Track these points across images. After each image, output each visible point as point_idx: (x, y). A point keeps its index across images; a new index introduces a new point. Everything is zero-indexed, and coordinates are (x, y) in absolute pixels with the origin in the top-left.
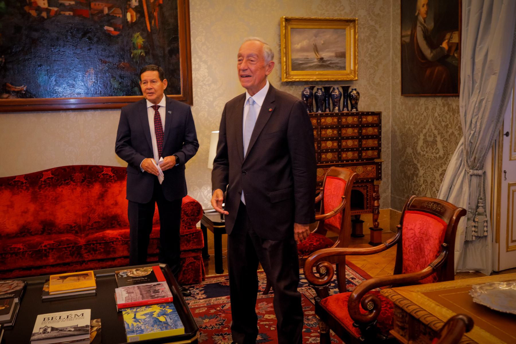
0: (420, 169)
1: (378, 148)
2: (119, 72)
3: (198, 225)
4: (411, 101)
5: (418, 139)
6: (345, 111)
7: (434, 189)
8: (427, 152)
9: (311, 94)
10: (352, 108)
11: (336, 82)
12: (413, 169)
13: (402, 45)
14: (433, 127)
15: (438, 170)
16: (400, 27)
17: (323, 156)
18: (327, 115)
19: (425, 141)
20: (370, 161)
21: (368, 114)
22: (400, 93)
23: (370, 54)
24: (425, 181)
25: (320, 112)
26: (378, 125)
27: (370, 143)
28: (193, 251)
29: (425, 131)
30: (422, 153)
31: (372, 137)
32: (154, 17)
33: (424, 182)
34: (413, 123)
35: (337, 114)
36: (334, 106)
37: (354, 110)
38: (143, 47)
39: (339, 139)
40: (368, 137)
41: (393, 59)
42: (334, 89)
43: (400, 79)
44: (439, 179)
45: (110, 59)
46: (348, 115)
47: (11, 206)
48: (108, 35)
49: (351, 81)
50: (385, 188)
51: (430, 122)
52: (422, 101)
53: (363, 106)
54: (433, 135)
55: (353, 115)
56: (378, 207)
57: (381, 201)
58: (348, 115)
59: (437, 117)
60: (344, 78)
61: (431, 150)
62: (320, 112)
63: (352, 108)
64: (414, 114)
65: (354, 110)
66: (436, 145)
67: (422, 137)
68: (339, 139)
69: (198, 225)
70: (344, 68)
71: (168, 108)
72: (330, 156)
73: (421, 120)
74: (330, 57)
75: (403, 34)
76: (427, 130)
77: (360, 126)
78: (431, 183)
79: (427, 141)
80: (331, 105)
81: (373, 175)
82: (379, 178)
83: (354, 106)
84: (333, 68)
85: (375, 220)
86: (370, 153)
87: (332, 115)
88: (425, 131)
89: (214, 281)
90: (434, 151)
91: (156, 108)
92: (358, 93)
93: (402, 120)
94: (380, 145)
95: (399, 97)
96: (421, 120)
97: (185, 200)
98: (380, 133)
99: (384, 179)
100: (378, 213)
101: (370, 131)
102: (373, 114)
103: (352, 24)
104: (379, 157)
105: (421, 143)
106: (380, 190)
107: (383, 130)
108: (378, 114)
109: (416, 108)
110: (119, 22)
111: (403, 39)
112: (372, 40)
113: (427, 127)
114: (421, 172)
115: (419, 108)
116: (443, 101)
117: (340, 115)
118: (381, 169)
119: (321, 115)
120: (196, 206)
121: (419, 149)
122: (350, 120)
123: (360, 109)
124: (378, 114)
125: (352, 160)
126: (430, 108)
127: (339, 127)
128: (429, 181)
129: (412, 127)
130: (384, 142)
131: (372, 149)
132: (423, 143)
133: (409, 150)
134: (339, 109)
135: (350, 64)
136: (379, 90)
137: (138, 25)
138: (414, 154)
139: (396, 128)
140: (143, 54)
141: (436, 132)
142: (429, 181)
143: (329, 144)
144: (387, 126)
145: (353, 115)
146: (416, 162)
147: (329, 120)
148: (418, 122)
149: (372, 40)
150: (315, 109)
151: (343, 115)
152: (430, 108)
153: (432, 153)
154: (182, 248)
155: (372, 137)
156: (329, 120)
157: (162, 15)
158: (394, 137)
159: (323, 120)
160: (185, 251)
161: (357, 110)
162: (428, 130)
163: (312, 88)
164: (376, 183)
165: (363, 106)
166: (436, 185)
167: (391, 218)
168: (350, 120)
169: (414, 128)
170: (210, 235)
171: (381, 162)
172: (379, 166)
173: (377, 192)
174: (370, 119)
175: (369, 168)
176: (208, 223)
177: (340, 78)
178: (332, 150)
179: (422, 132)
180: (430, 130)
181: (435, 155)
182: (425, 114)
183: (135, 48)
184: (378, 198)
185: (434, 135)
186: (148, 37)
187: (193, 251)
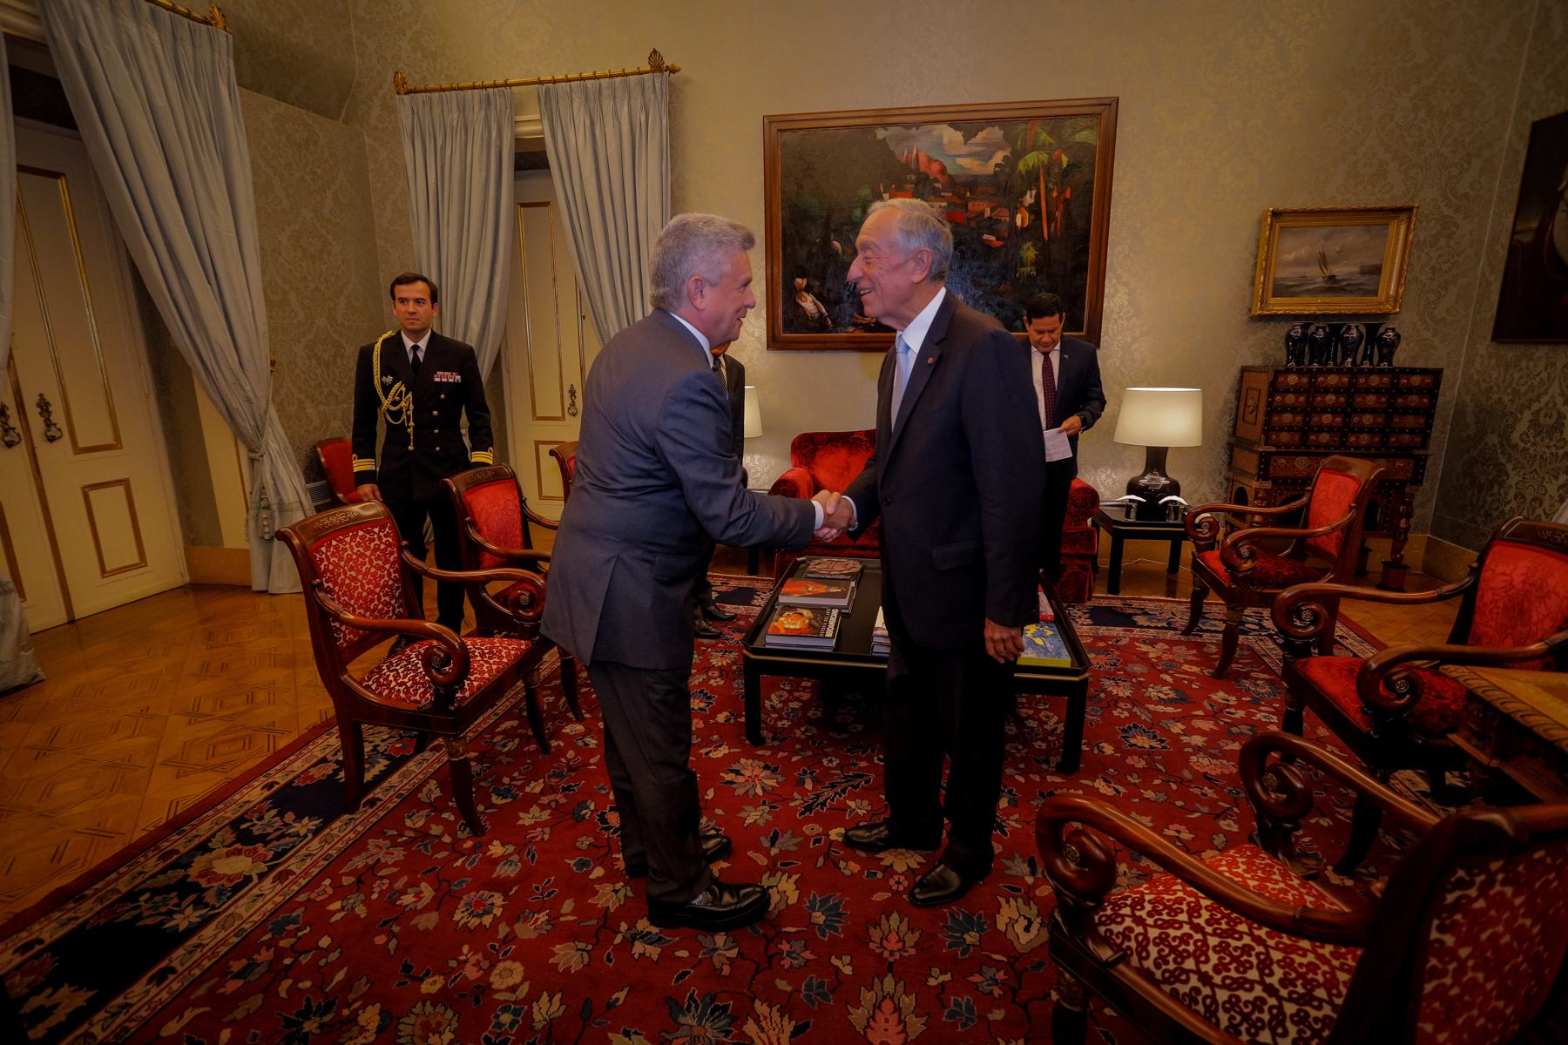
0: (1512, 474)
1: (1424, 433)
2: (998, 299)
3: (1089, 521)
4: (1510, 353)
5: (1517, 420)
6: (1366, 365)
7: (1539, 511)
9: (1304, 334)
10: (1381, 361)
11: (1355, 316)
13: (1513, 249)
14: (1559, 400)
15: (1557, 478)
16: (1512, 215)
17: (1313, 437)
18: (1330, 372)
19: (1534, 423)
20: (1404, 452)
21: (1413, 371)
22: (1489, 337)
23: (1433, 268)
24: (1520, 496)
25: (1316, 365)
26: (1432, 391)
27: (1410, 421)
28: (1079, 556)
29: (1536, 406)
30: (1522, 445)
31: (1416, 411)
32: (1055, 219)
35: (1349, 371)
36: (1344, 359)
37: (1384, 365)
38: (1035, 263)
39: (1347, 411)
40: (1406, 411)
41: (1483, 274)
42: (1349, 328)
43: (1494, 311)
44: (1556, 495)
45: (987, 281)
46: (1371, 372)
47: (848, 469)
48: (987, 247)
49: (1385, 316)
50: (1426, 499)
51: (1555, 389)
52: (1542, 351)
53: (1401, 358)
54: (1555, 415)
55: (1381, 372)
56: (1407, 529)
57: (1413, 521)
58: (1371, 372)
60: (1373, 310)
62: (1316, 365)
63: (1381, 361)
64: (1517, 376)
65: (1384, 365)
67: (1527, 416)
68: (1347, 411)
69: (1089, 521)
70: (1375, 293)
71: (1062, 352)
72: (1324, 437)
73: (1532, 388)
74: (1351, 273)
75: (1518, 228)
77: (1394, 391)
78: (1534, 500)
80: (1339, 355)
82: (1417, 479)
83: (1387, 357)
84: (1351, 292)
86: (1406, 438)
87: (1340, 372)
89: (1105, 603)
91: (1046, 354)
93: (1484, 386)
94: (1429, 426)
95: (1484, 345)
96: (1532, 388)
97: (1075, 484)
98: (1433, 406)
99: (1426, 485)
100: (1406, 539)
101: (1413, 400)
102: (1424, 372)
103: (1403, 216)
104: (1424, 445)
105: (1522, 427)
106: (1415, 503)
107: (1440, 400)
108: (1437, 374)
109: (1524, 364)
110: (1004, 228)
111: (1517, 237)
112: (1442, 242)
113: (1544, 399)
114: (1514, 478)
117: (1355, 372)
118: (1424, 467)
119: (1319, 371)
120: (1091, 496)
121: (1515, 437)
122: (1375, 380)
123: (1395, 363)
124: (1437, 374)
125: (1367, 447)
126: (1559, 366)
127: (1350, 391)
128: (1530, 494)
129: (1506, 398)
130: (1437, 422)
131: (1412, 431)
133: (1492, 439)
134: (1354, 363)
135: (1389, 285)
136: (1443, 328)
137: (1031, 232)
139: (1468, 399)
140: (1034, 273)
142: (1530, 494)
143: (1327, 419)
144: (1448, 395)
145: (1381, 372)
146: (1503, 460)
147: (1333, 380)
148: (1523, 389)
149: (1442, 242)
150: (1306, 361)
151: (1361, 372)
152: (1559, 366)
154: (1063, 551)
155: (1416, 411)
156: (1333, 380)
157: (1067, 214)
158: (1460, 412)
159: (1321, 379)
160: (1067, 555)
161: (1390, 363)
163: (1305, 327)
164: (1407, 490)
165: (1401, 358)
166: (1546, 504)
167: (1427, 552)
168: (1375, 380)
169: (1512, 401)
170: (1105, 539)
171: (1426, 456)
172: (1420, 464)
173: (1410, 505)
174: (1416, 380)
175: (1399, 464)
176: (1104, 521)
177: (1363, 309)
178: (1330, 429)
182: (1544, 375)
183: (1023, 265)
184: (1409, 515)
185: (1559, 413)
186: (1044, 248)
187: (1079, 556)
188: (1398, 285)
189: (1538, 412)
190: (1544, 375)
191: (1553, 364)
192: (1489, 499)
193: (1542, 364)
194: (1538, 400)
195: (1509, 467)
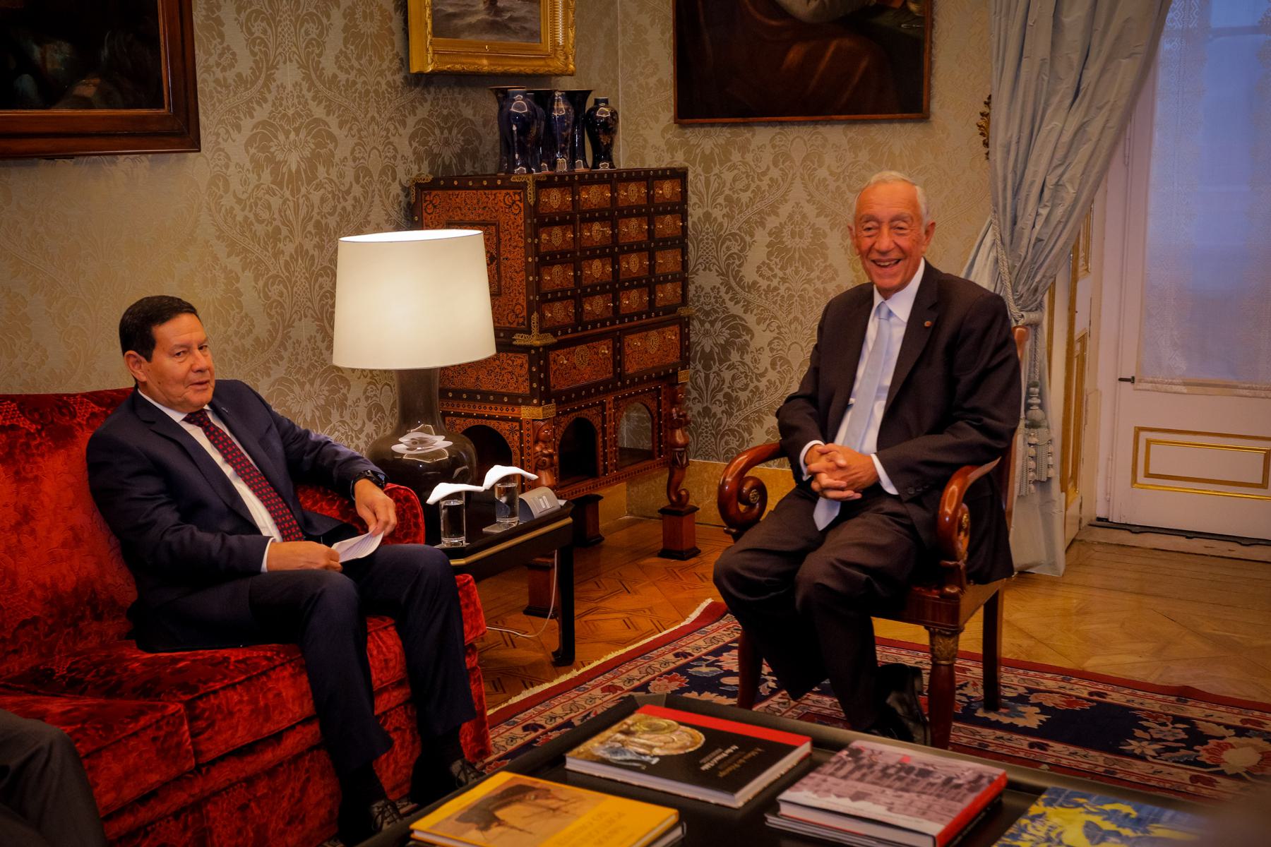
8: (784, 280)
12: (726, 333)
29: (772, 222)
33: (773, 365)
34: (721, 200)
54: (808, 232)
59: (825, 179)
61: (804, 271)
65: (604, 167)
66: (826, 258)
76: (783, 218)
79: (787, 250)
81: (673, 358)
83: (604, 152)
85: (673, 487)
88: (772, 222)
90: (813, 275)
92: (614, 113)
109: (736, 157)
113: (785, 210)
115: (749, 157)
116: (850, 134)
121: (749, 274)
129: (717, 213)
132: (769, 254)
138: (730, 288)
141: (823, 223)
145: (600, 180)
146: (737, 310)
148: (745, 197)
153: (809, 281)
161: (612, 166)
162: (790, 217)
165: (623, 158)
179: (763, 224)
180: (797, 218)
181: (819, 285)
188: (566, 26)
189: (777, 233)
190: (775, 173)
191: (787, 157)
192: (727, 375)
193: (767, 157)
194: (774, 211)
195: (751, 320)
